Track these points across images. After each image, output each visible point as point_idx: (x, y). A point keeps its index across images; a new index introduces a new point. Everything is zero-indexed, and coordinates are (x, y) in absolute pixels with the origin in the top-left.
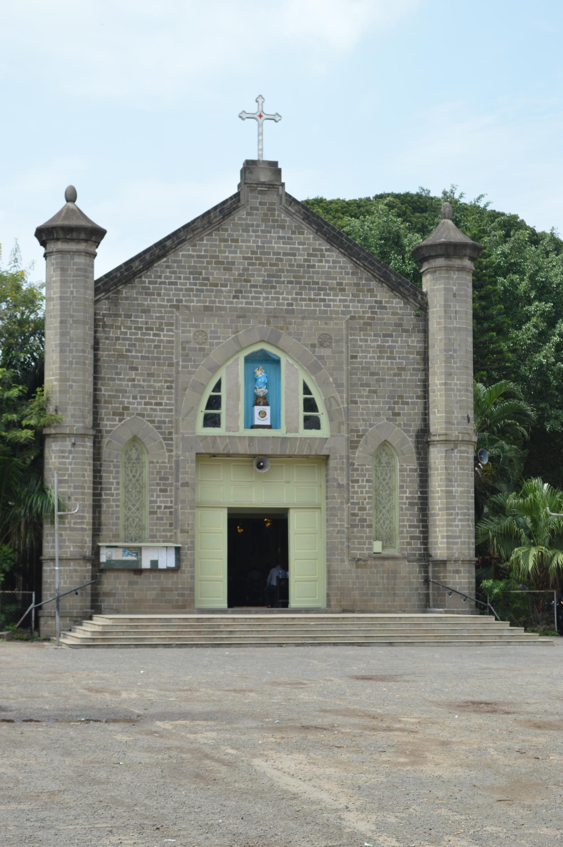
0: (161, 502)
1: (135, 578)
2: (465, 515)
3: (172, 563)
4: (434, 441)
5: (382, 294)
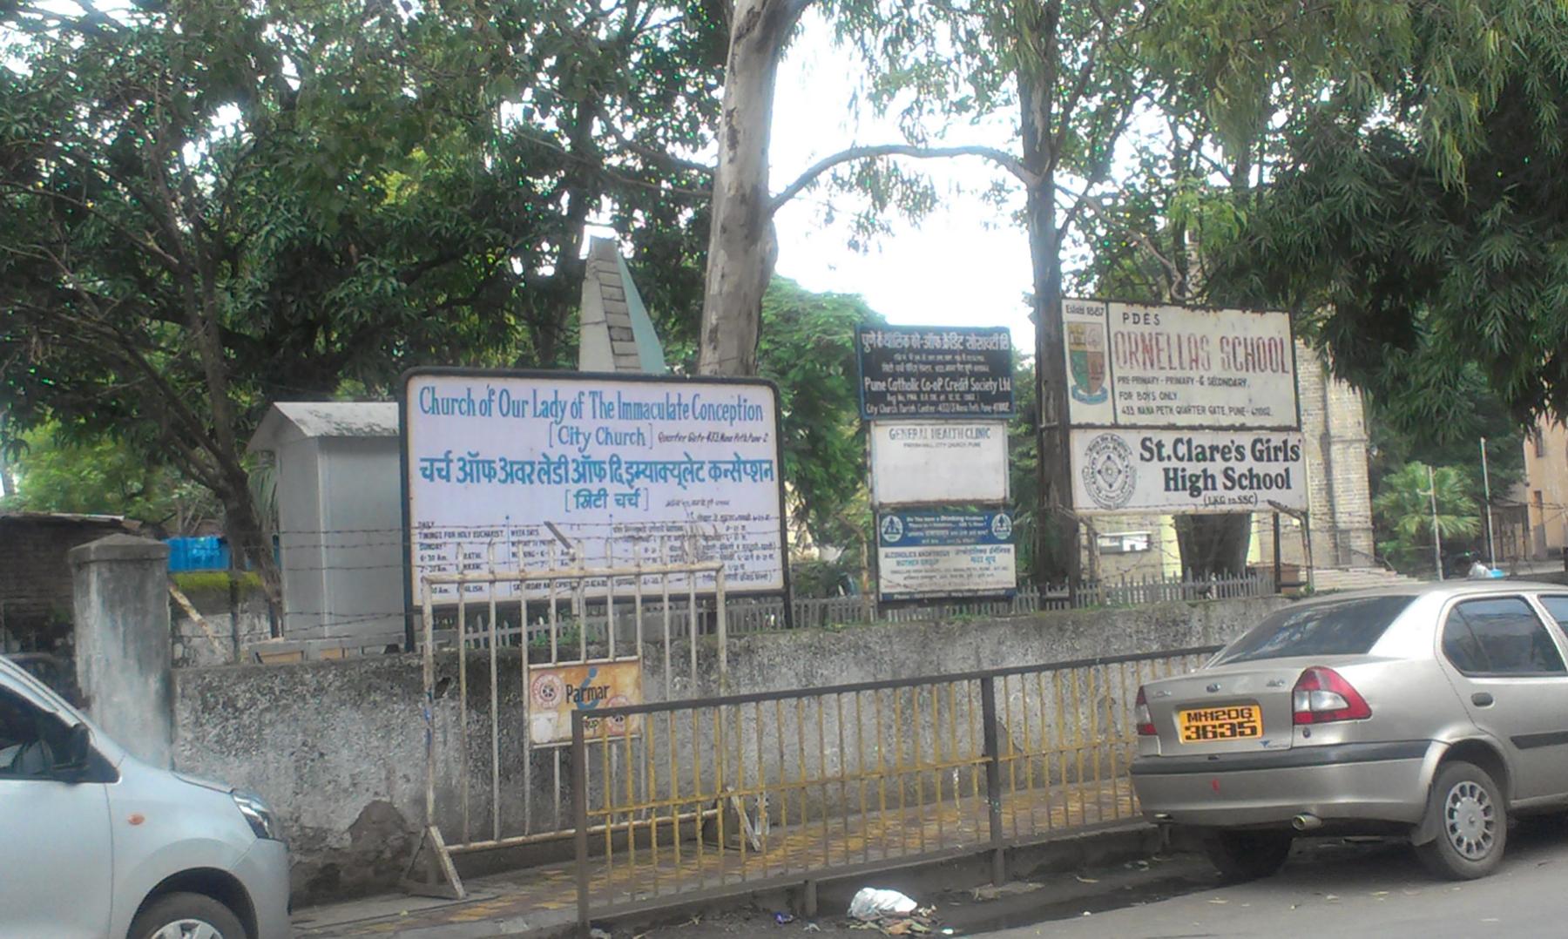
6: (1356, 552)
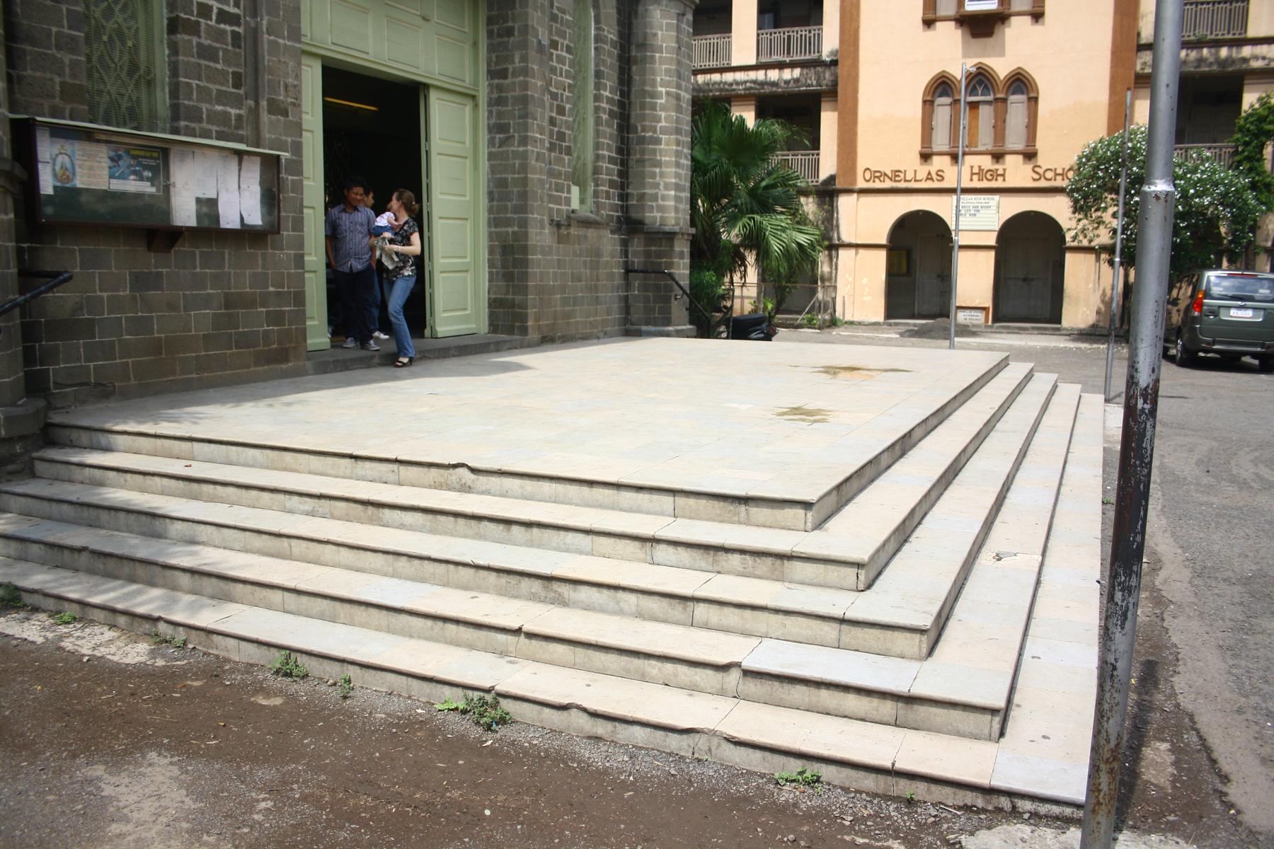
1: (152, 262)
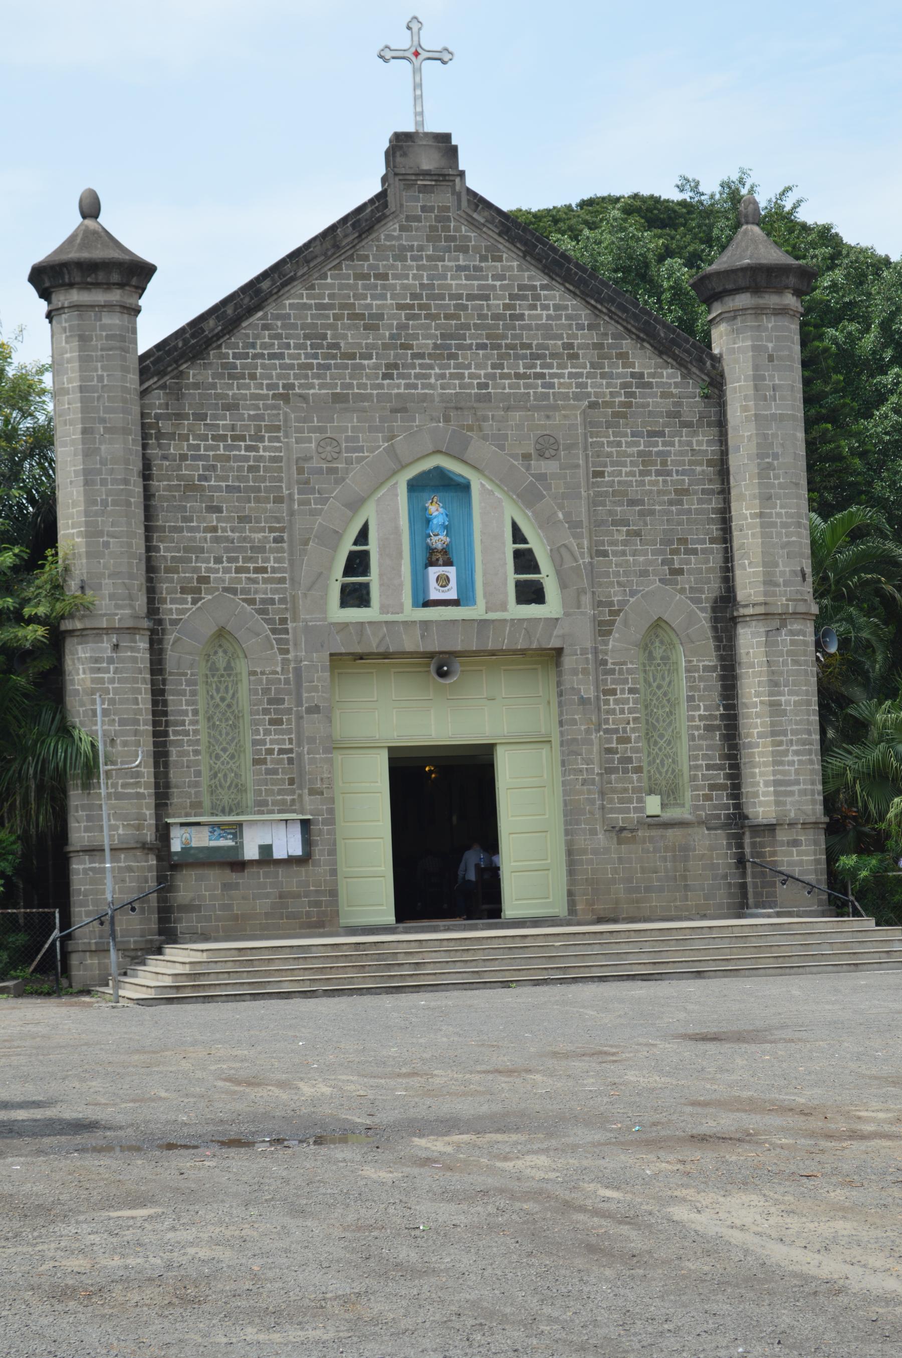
0: (272, 742)
1: (233, 877)
2: (804, 744)
3: (296, 849)
4: (744, 616)
5: (643, 361)
6: (788, 878)
